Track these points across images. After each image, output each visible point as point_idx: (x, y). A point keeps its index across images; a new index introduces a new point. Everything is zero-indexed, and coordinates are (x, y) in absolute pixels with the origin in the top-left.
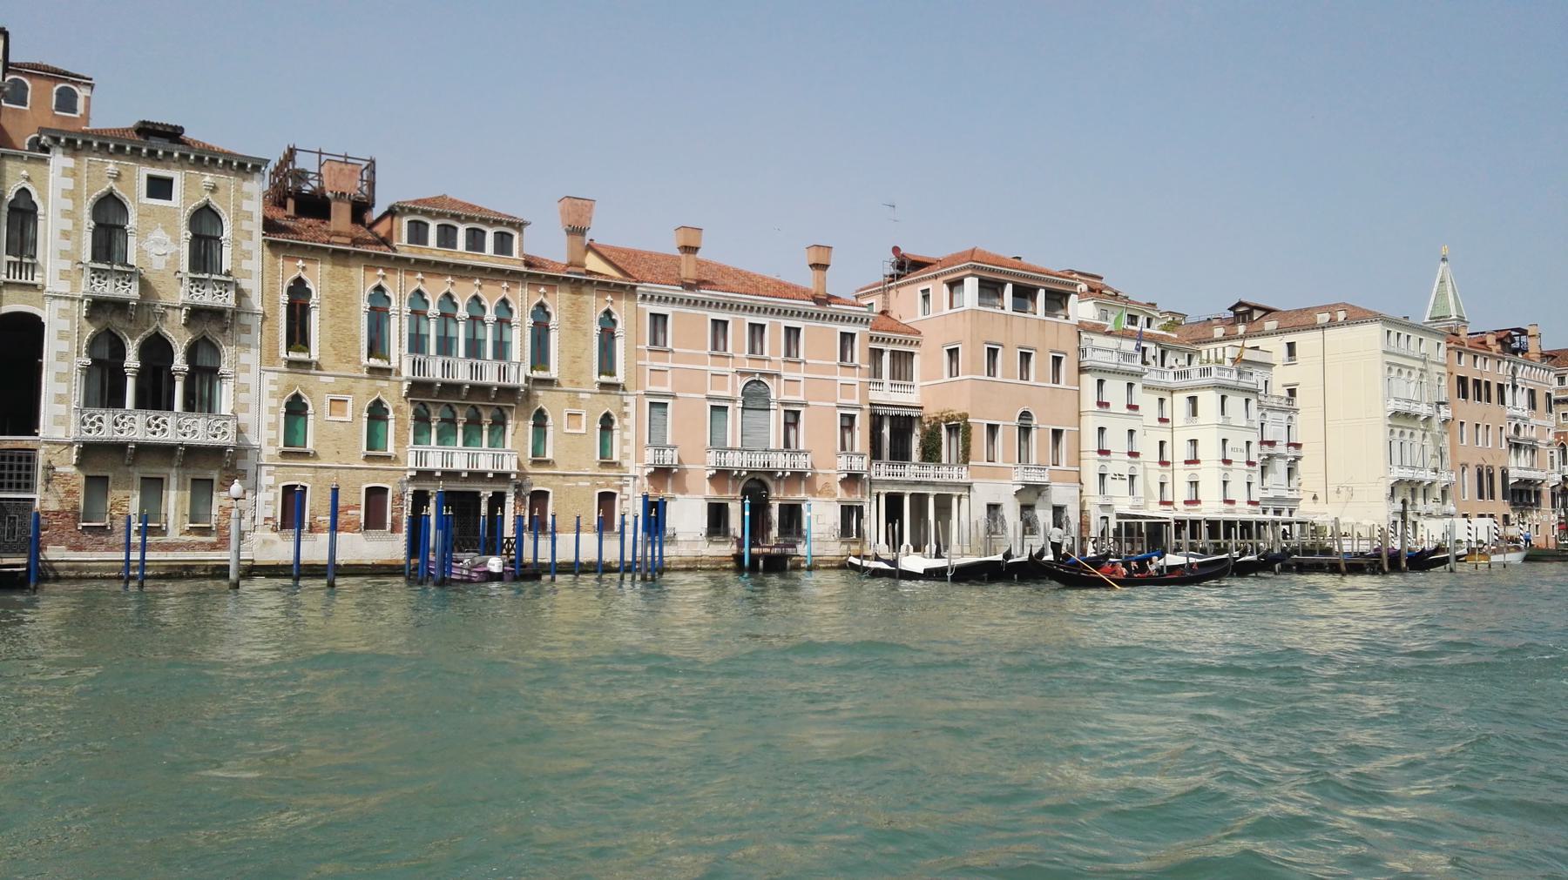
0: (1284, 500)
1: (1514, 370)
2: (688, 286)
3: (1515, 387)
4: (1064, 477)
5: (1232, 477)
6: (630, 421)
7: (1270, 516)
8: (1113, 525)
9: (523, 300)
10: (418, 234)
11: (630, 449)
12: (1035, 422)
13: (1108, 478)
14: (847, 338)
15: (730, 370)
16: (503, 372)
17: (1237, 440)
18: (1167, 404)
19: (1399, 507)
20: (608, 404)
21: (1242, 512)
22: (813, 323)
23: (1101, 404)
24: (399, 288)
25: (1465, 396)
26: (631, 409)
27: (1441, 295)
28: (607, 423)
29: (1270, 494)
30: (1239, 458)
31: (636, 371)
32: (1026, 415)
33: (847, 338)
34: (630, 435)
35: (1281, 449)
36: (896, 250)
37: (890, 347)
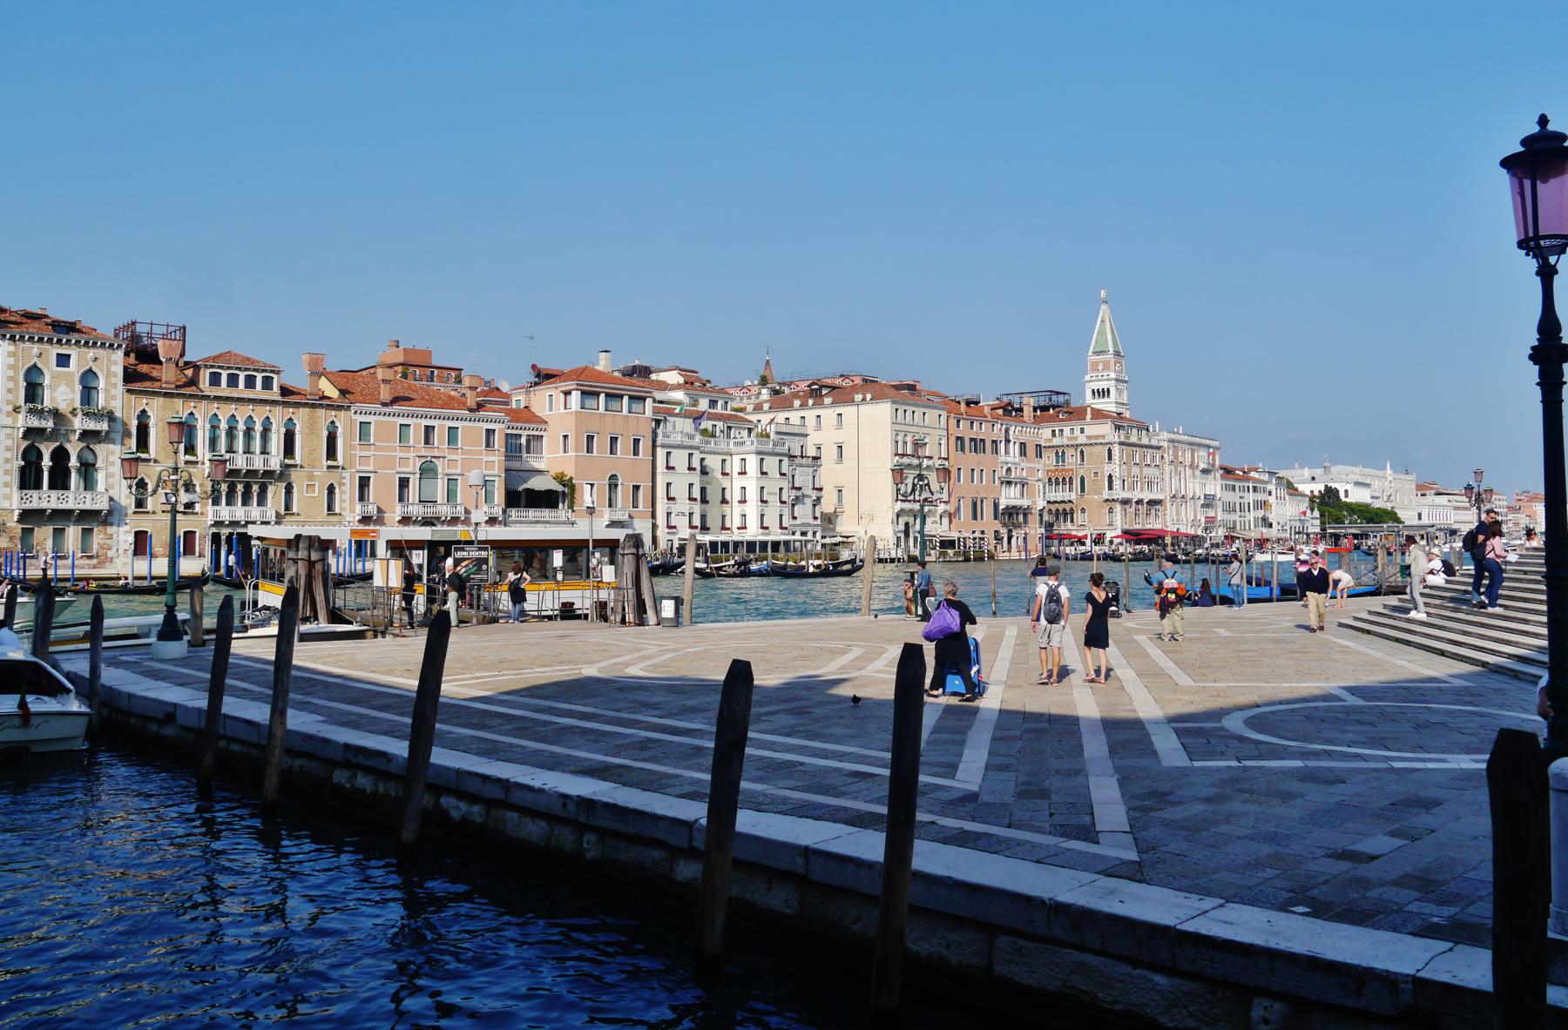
0: (809, 525)
1: (1007, 431)
2: (384, 404)
3: (1008, 441)
5: (766, 511)
6: (346, 488)
7: (798, 537)
8: (676, 545)
9: (278, 417)
10: (215, 380)
11: (346, 505)
14: (490, 432)
15: (411, 455)
16: (266, 462)
17: (772, 486)
18: (728, 463)
19: (902, 527)
20: (332, 478)
21: (776, 535)
22: (467, 424)
23: (668, 468)
24: (202, 416)
25: (963, 450)
26: (347, 481)
27: (1102, 332)
28: (331, 490)
29: (798, 522)
30: (773, 500)
31: (349, 458)
32: (613, 477)
33: (490, 432)
34: (346, 497)
35: (808, 491)
36: (534, 367)
37: (525, 433)
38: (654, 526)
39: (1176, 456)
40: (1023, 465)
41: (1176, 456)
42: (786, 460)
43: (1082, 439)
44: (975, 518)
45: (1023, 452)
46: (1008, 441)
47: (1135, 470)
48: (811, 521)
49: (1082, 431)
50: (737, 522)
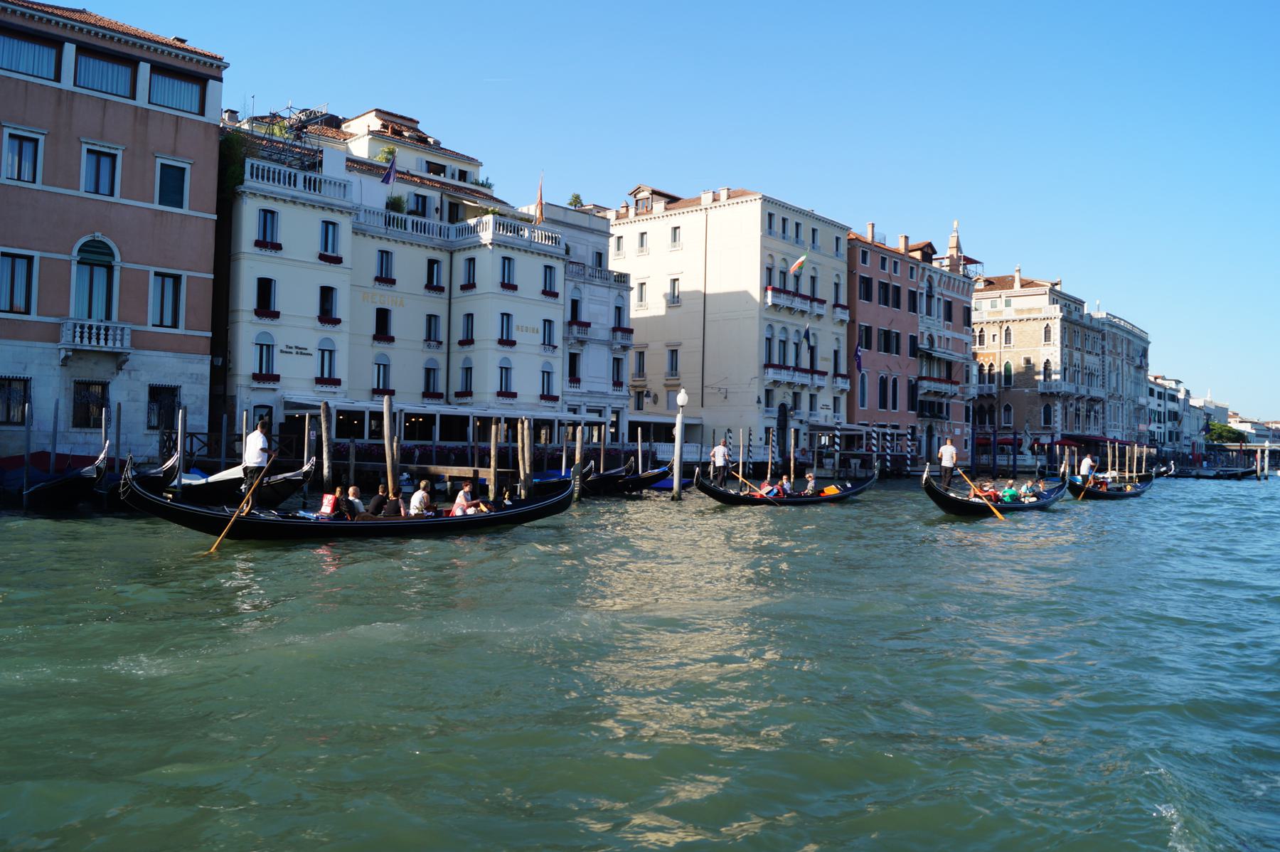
3: (930, 296)
4: (179, 347)
12: (118, 258)
13: (276, 351)
25: (868, 297)
38: (221, 376)
39: (1115, 346)
40: (948, 334)
41: (1115, 346)
42: (559, 267)
43: (1009, 314)
44: (883, 404)
45: (949, 317)
46: (930, 296)
47: (1077, 355)
48: (609, 388)
49: (1008, 304)
50: (457, 385)
